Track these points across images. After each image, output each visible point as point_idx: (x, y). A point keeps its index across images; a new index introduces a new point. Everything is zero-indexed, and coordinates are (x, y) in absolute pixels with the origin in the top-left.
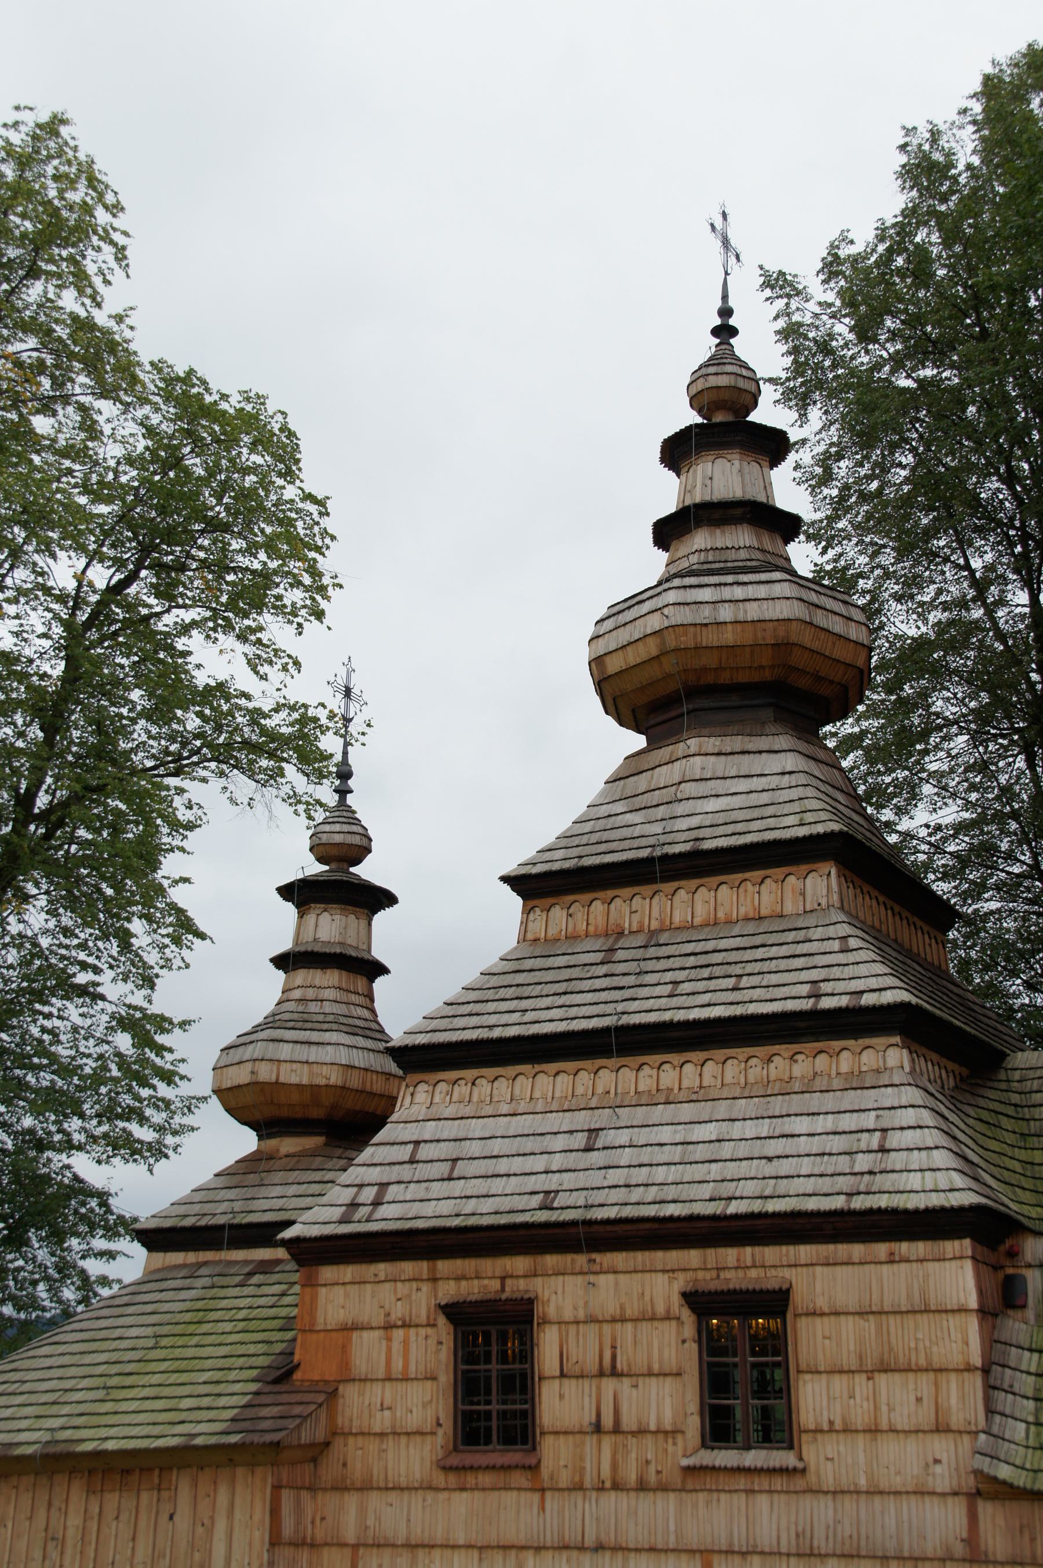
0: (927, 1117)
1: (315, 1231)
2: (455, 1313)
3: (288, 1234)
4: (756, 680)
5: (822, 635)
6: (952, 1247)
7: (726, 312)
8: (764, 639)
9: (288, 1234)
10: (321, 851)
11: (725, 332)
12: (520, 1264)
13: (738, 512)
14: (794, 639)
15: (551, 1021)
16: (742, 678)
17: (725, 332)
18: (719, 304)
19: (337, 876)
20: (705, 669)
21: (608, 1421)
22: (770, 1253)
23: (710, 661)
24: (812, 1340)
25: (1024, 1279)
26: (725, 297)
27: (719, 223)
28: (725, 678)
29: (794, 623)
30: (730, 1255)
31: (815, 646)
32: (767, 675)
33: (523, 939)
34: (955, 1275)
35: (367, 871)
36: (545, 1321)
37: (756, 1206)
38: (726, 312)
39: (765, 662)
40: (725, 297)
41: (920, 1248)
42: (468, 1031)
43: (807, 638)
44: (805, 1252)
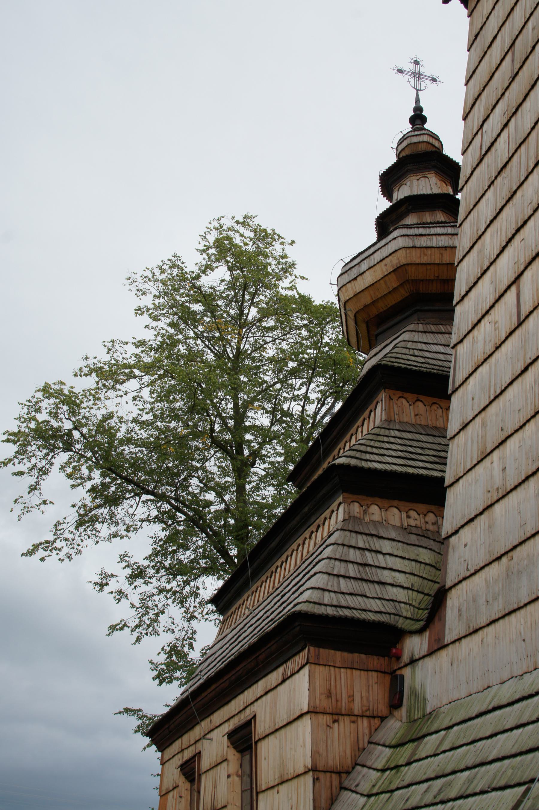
4: (399, 300)
5: (429, 252)
8: (387, 270)
11: (418, 118)
13: (403, 208)
14: (403, 261)
16: (391, 301)
17: (418, 118)
18: (414, 105)
20: (366, 306)
23: (366, 299)
25: (402, 677)
26: (417, 101)
27: (409, 67)
28: (382, 306)
29: (400, 251)
31: (424, 260)
32: (403, 293)
39: (395, 286)
40: (417, 101)
43: (415, 257)
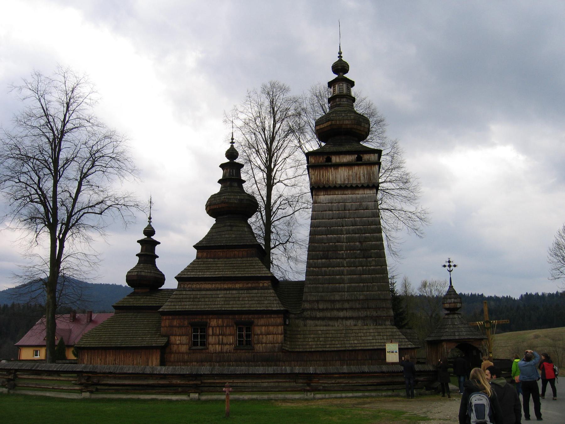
0: (276, 295)
1: (166, 310)
2: (192, 325)
3: (161, 310)
6: (280, 315)
7: (232, 139)
9: (161, 310)
10: (145, 232)
12: (204, 317)
15: (208, 274)
17: (232, 143)
19: (149, 239)
21: (220, 342)
22: (250, 316)
24: (257, 330)
30: (243, 316)
33: (197, 258)
34: (279, 320)
35: (154, 237)
36: (209, 327)
37: (249, 309)
38: (232, 139)
41: (276, 316)
42: (192, 274)
44: (256, 316)
